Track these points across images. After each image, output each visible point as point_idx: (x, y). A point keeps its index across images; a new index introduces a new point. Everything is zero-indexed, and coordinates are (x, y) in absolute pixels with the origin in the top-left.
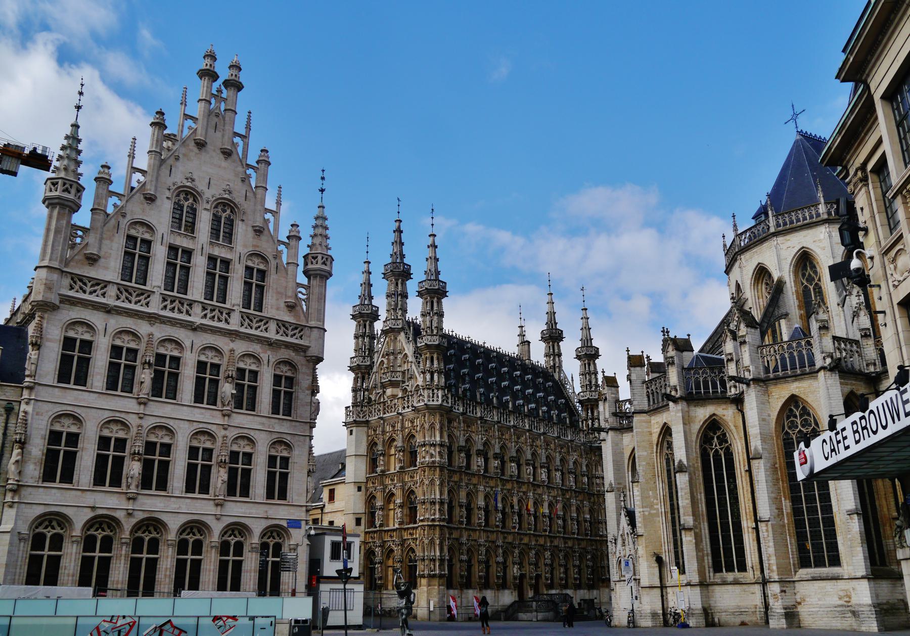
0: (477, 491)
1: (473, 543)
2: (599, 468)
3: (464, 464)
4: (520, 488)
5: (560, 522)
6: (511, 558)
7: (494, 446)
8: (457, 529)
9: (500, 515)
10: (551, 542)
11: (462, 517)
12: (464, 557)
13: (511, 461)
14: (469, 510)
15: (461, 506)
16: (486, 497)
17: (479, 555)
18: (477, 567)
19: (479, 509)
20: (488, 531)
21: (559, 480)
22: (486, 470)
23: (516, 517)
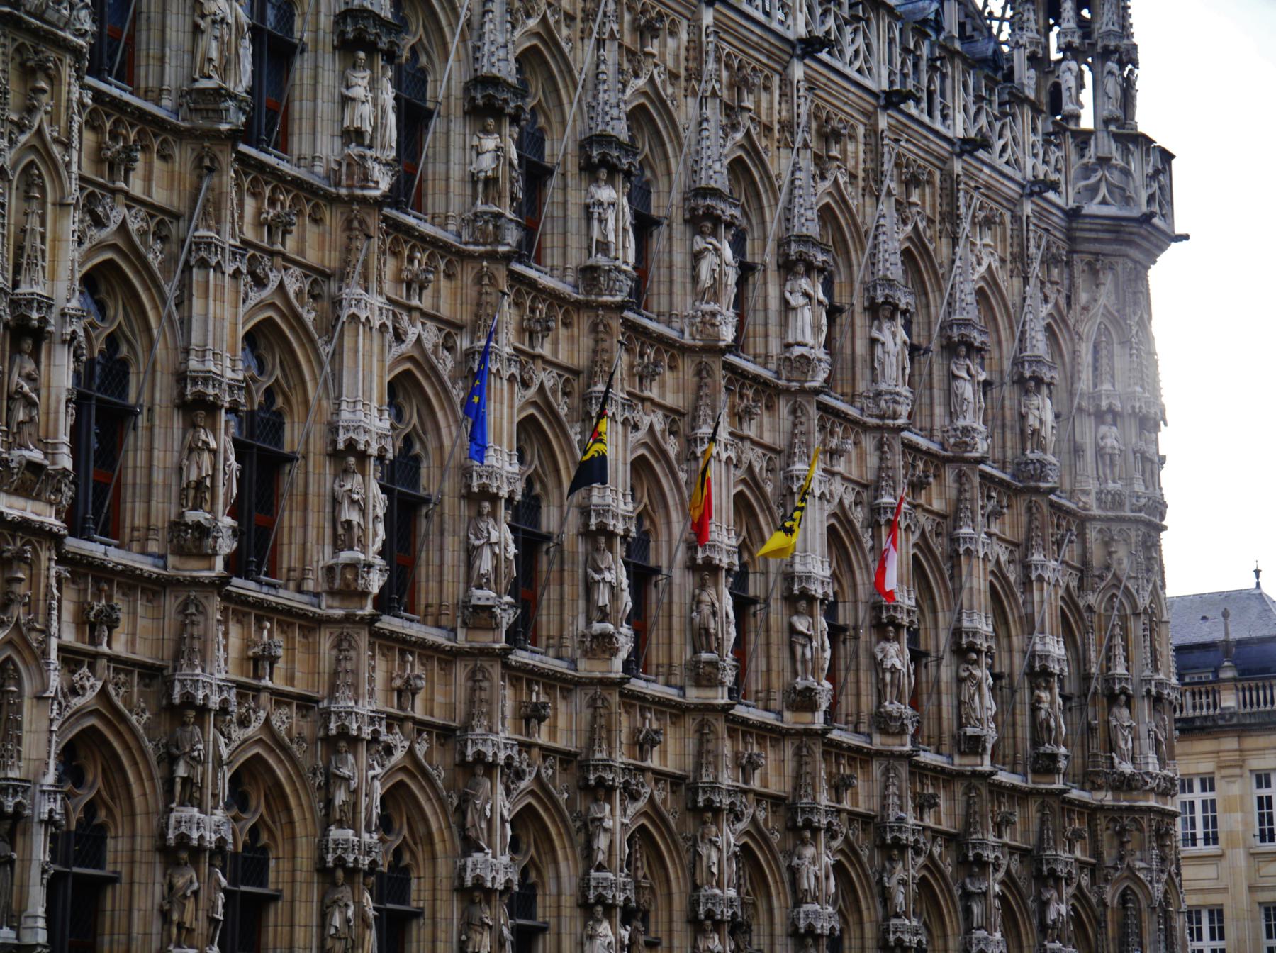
0: (330, 326)
1: (284, 720)
2: (1120, 361)
3: (241, 81)
4: (645, 375)
5: (896, 655)
6: (568, 870)
7: (474, 29)
8: (154, 587)
9: (501, 534)
10: (840, 786)
11: (199, 492)
12: (209, 824)
13: (590, 170)
14: (264, 465)
15: (196, 409)
16: (402, 390)
17: (329, 818)
18: (306, 913)
19: (347, 456)
20: (403, 645)
21: (893, 378)
22: (407, 190)
23: (616, 573)
